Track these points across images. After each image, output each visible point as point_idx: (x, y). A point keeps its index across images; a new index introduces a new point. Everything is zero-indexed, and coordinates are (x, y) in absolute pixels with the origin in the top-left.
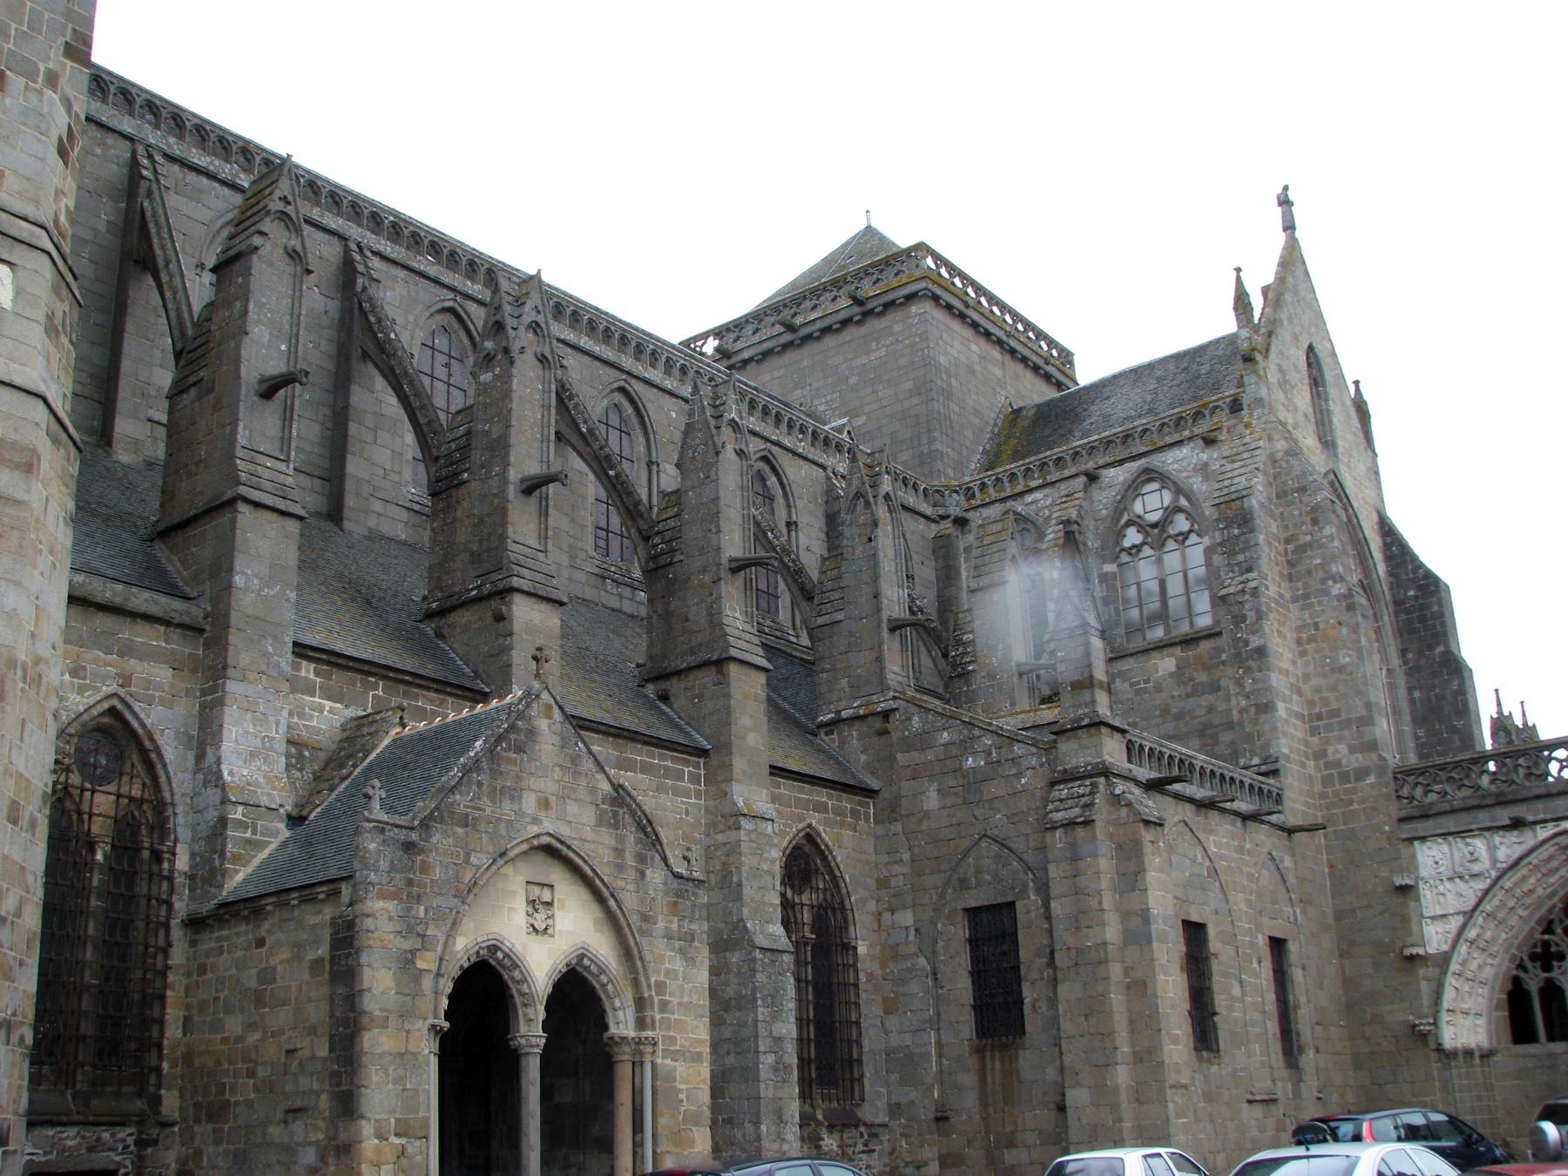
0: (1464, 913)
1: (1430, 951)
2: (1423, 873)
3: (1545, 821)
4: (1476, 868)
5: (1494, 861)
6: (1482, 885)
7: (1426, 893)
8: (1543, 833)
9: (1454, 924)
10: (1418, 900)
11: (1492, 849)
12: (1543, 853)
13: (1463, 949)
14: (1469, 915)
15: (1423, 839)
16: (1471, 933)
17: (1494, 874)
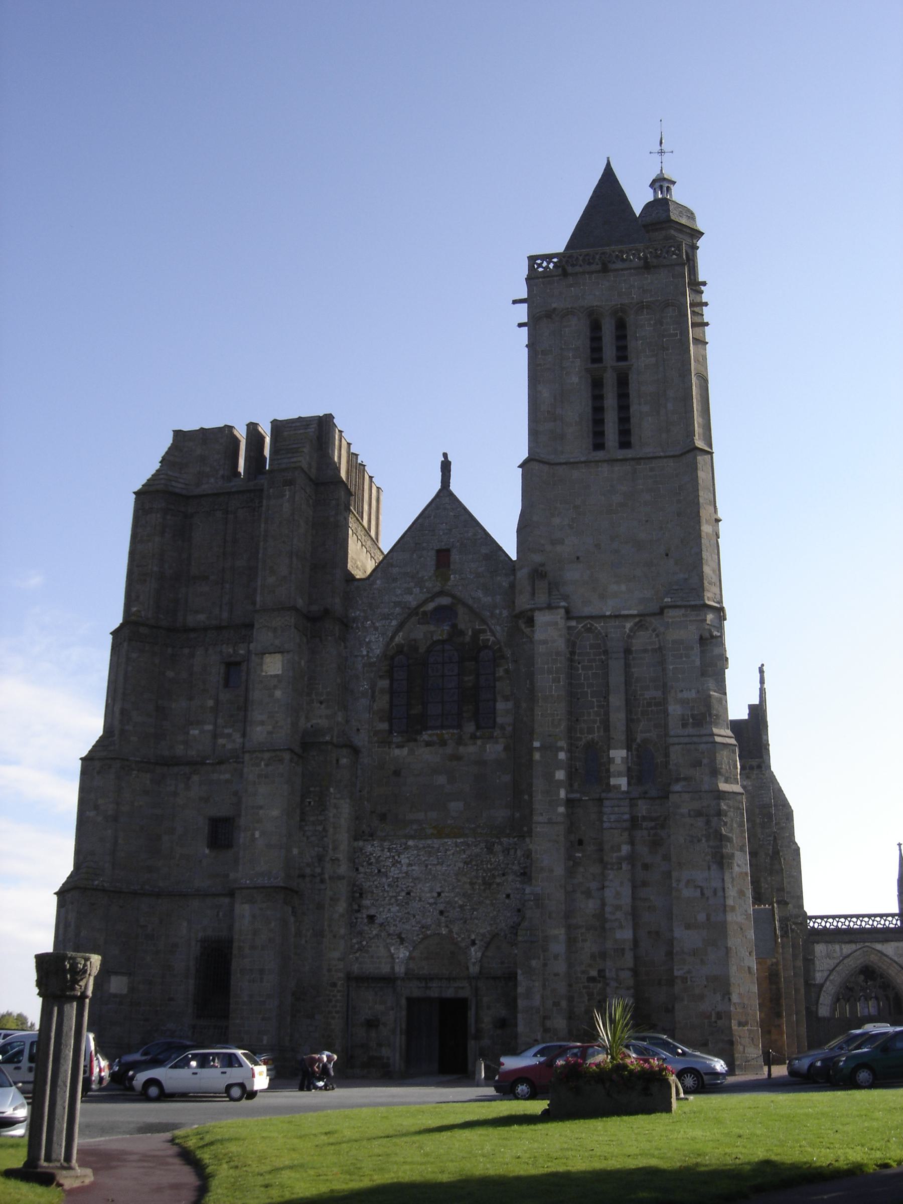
0: (829, 970)
1: (817, 982)
2: (816, 954)
3: (860, 942)
4: (835, 955)
5: (842, 953)
6: (837, 961)
7: (817, 962)
8: (859, 946)
9: (826, 974)
10: (814, 964)
11: (841, 949)
12: (858, 953)
13: (828, 983)
14: (831, 971)
15: (818, 943)
16: (831, 978)
17: (841, 958)
